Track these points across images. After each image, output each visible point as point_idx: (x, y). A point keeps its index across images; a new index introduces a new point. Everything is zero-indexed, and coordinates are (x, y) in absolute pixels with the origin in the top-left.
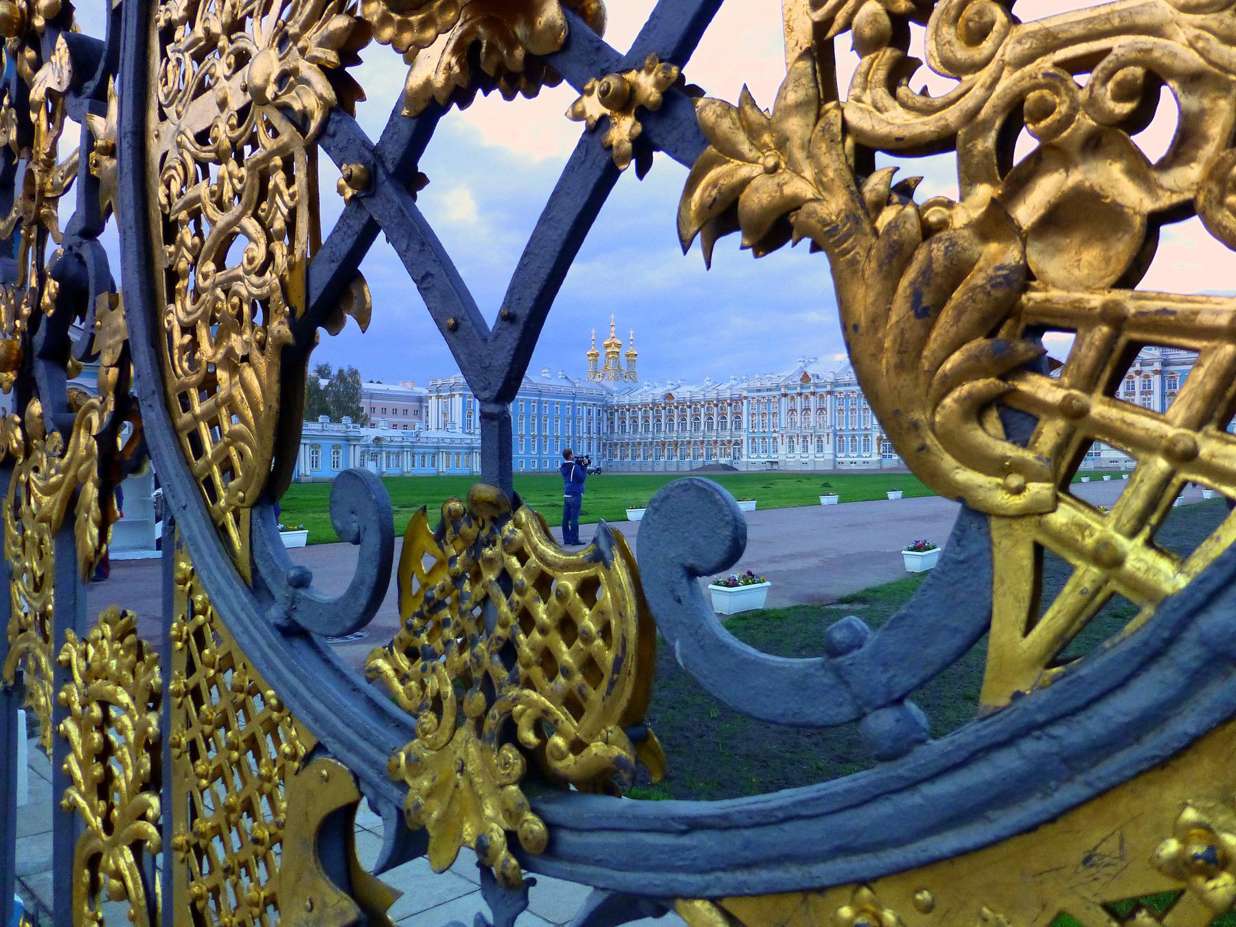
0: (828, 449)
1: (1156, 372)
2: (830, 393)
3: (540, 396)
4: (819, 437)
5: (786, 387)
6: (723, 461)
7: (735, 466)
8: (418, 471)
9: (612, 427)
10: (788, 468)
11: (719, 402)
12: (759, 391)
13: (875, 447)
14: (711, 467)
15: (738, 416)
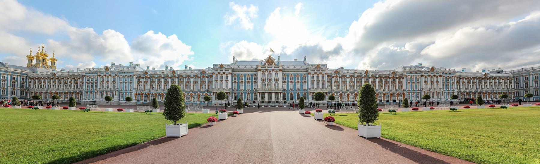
1: (230, 73)
2: (117, 75)
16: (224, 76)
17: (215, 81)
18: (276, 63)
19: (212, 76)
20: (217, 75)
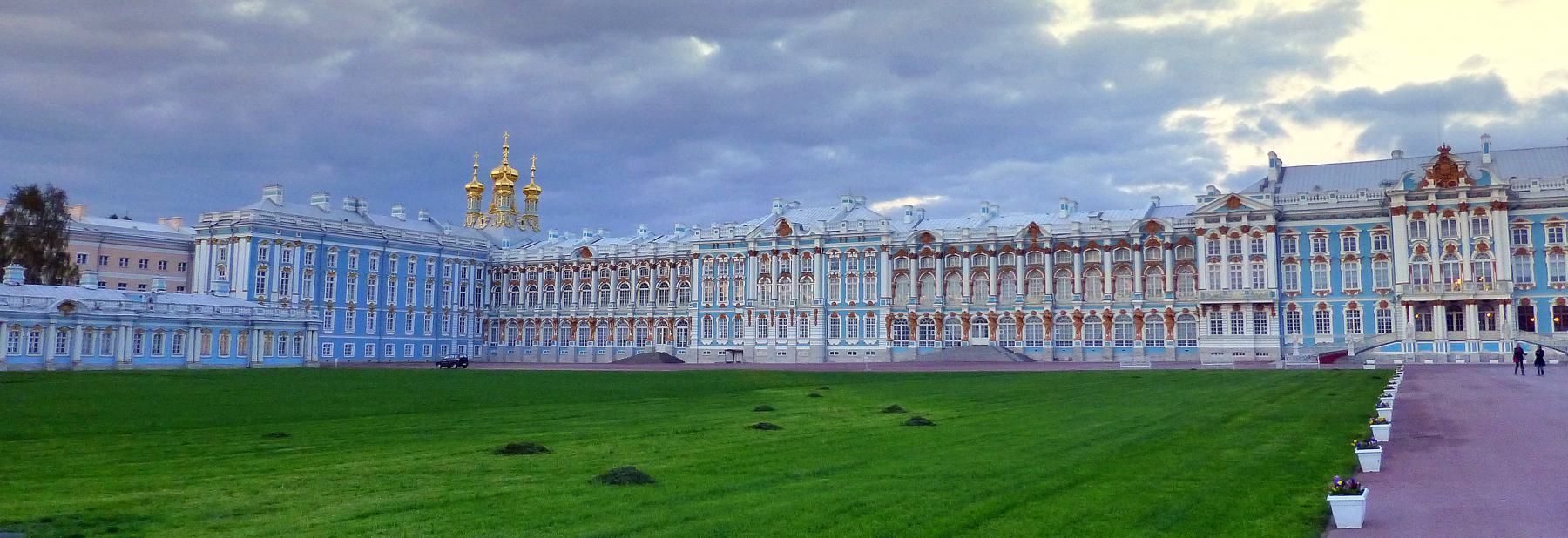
0: (816, 332)
1: (1269, 229)
2: (818, 251)
3: (385, 245)
4: (803, 315)
5: (755, 241)
6: (662, 348)
7: (679, 356)
8: (148, 360)
9: (498, 297)
10: (758, 361)
11: (659, 261)
12: (716, 246)
13: (884, 331)
14: (644, 359)
15: (684, 281)
16: (1245, 239)
17: (1209, 259)
18: (1477, 176)
19: (1194, 243)
20: (1214, 237)
